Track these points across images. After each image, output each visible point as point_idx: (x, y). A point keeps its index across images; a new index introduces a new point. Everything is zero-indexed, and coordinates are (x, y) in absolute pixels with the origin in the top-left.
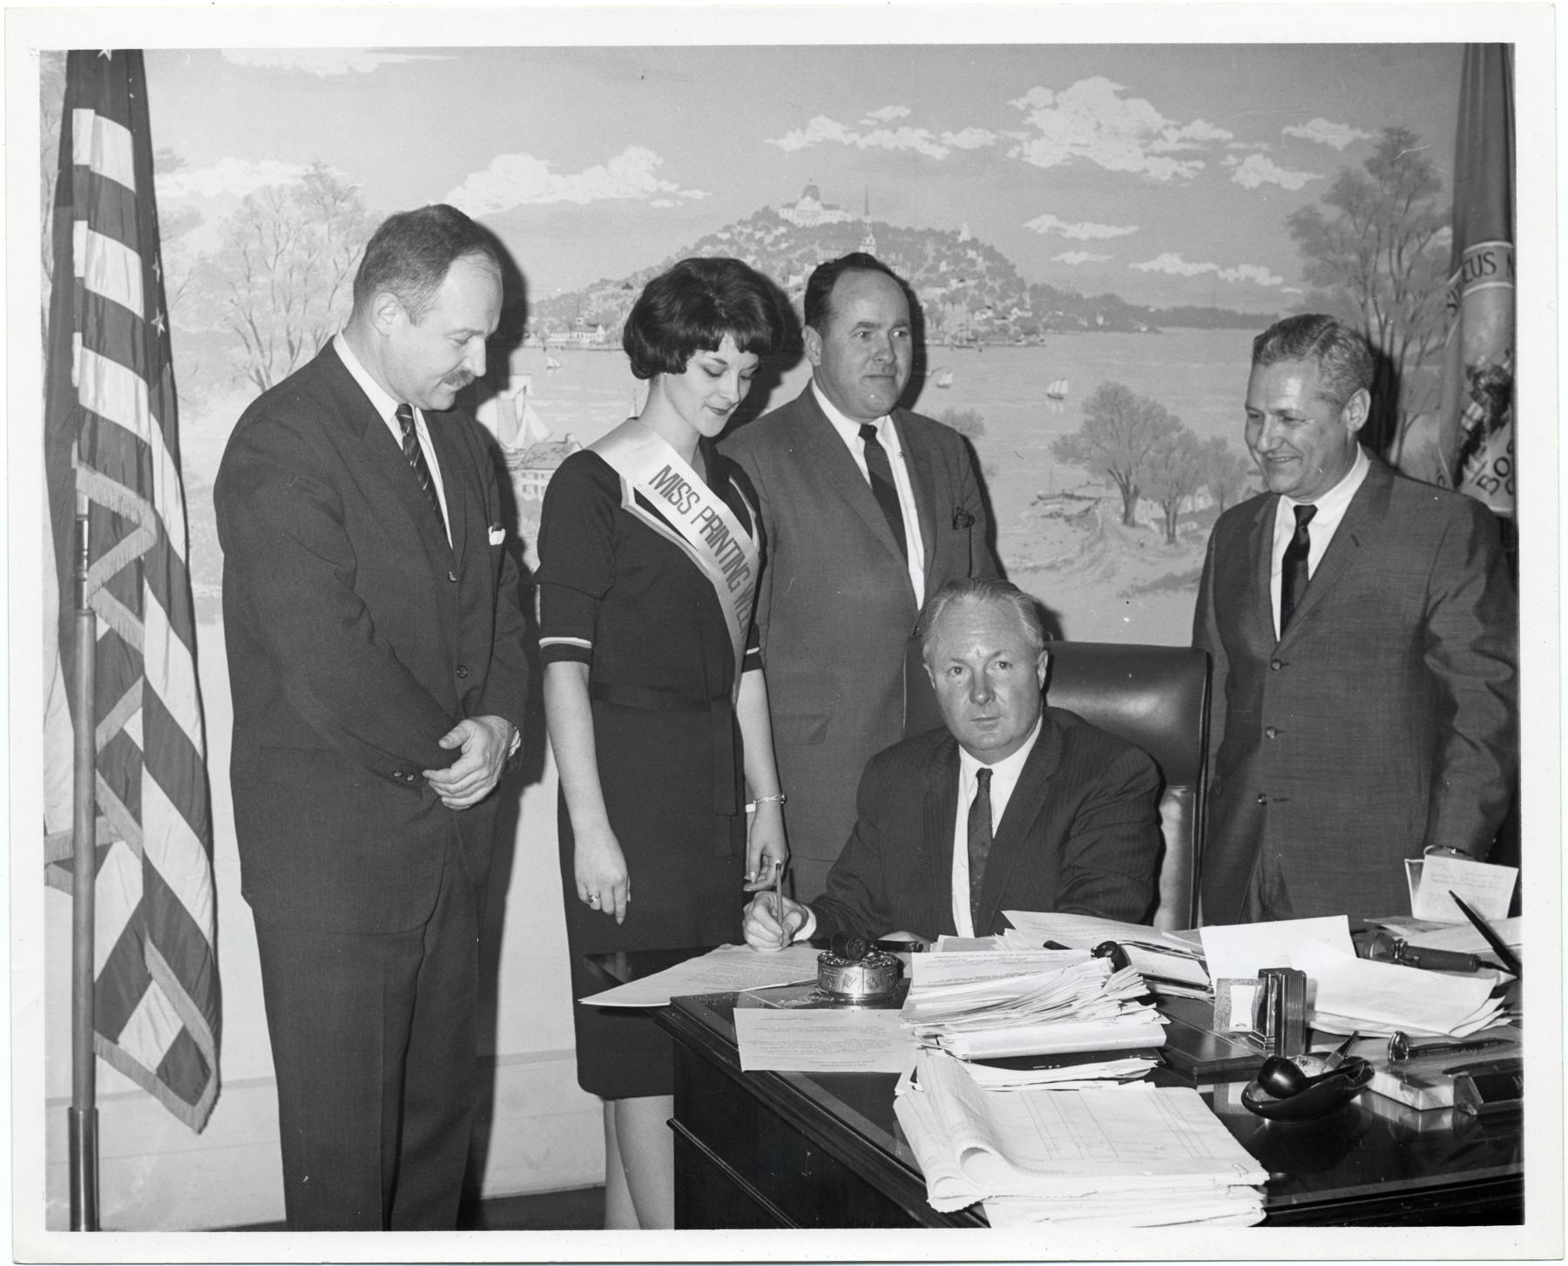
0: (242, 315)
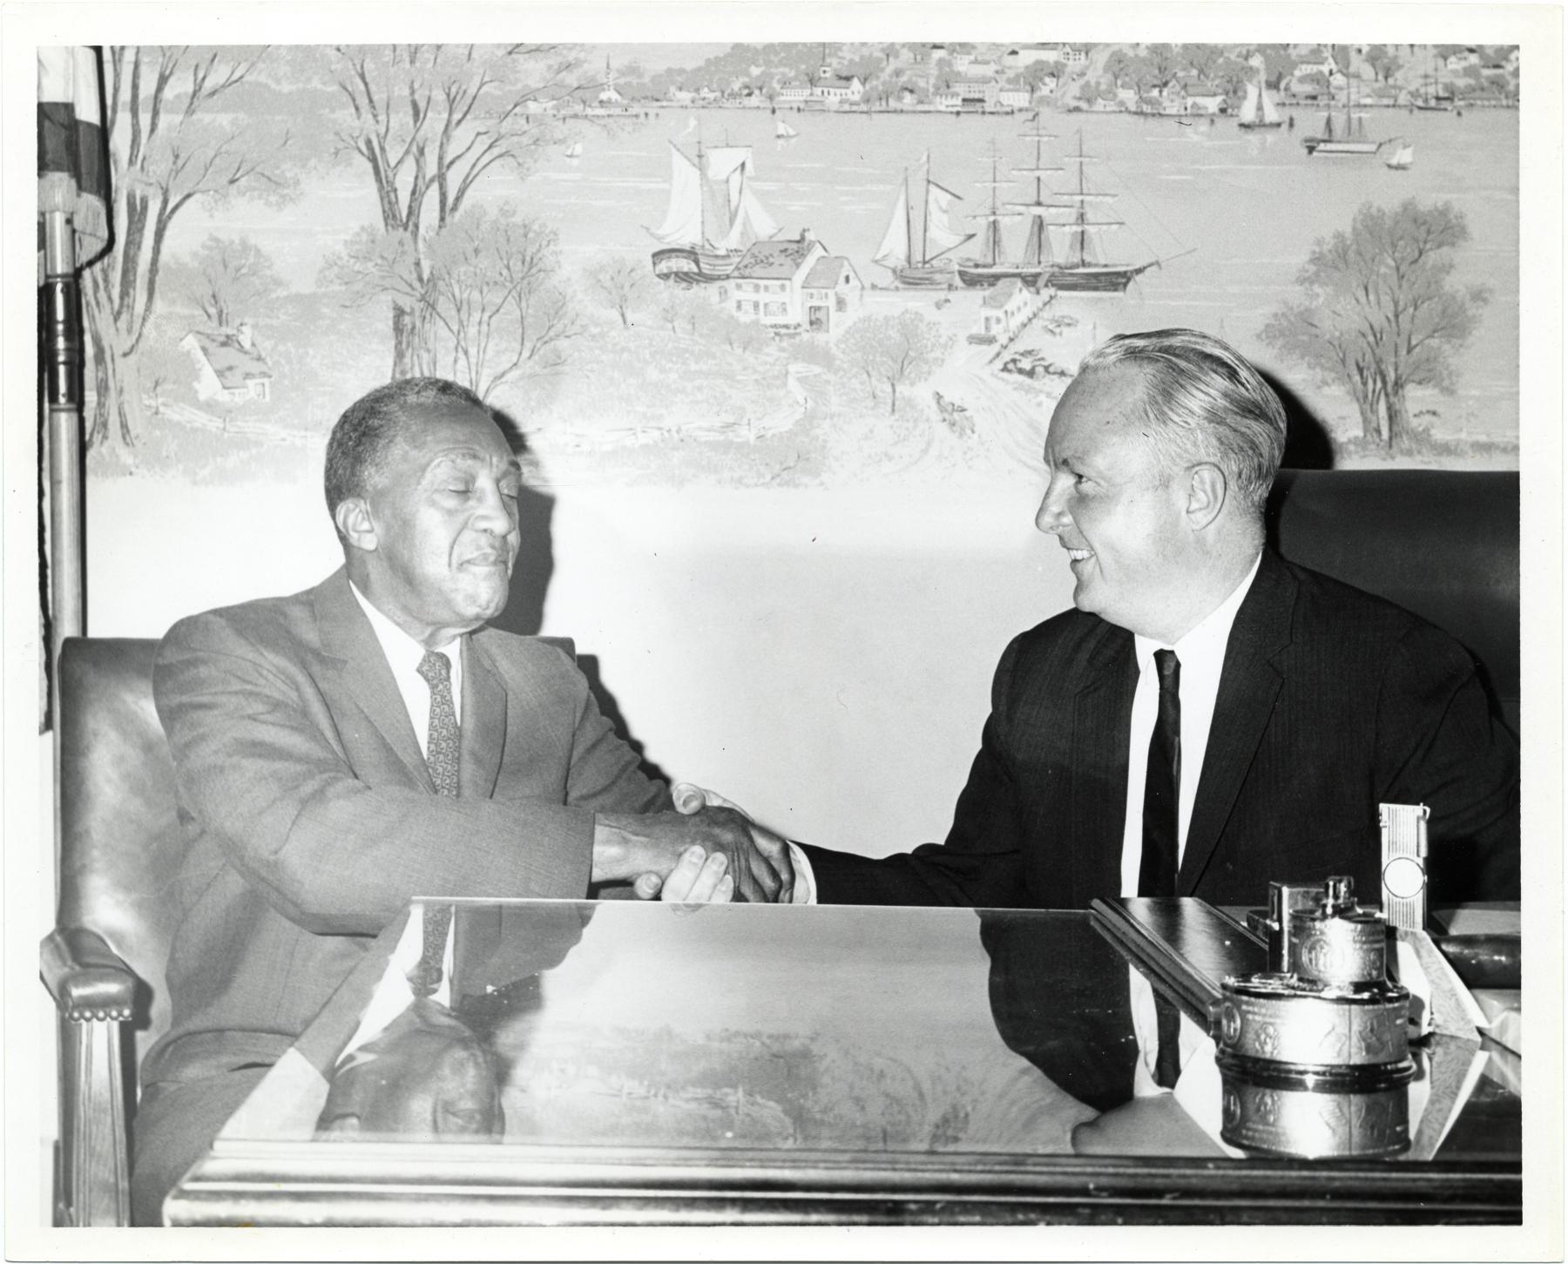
0: (351, 67)
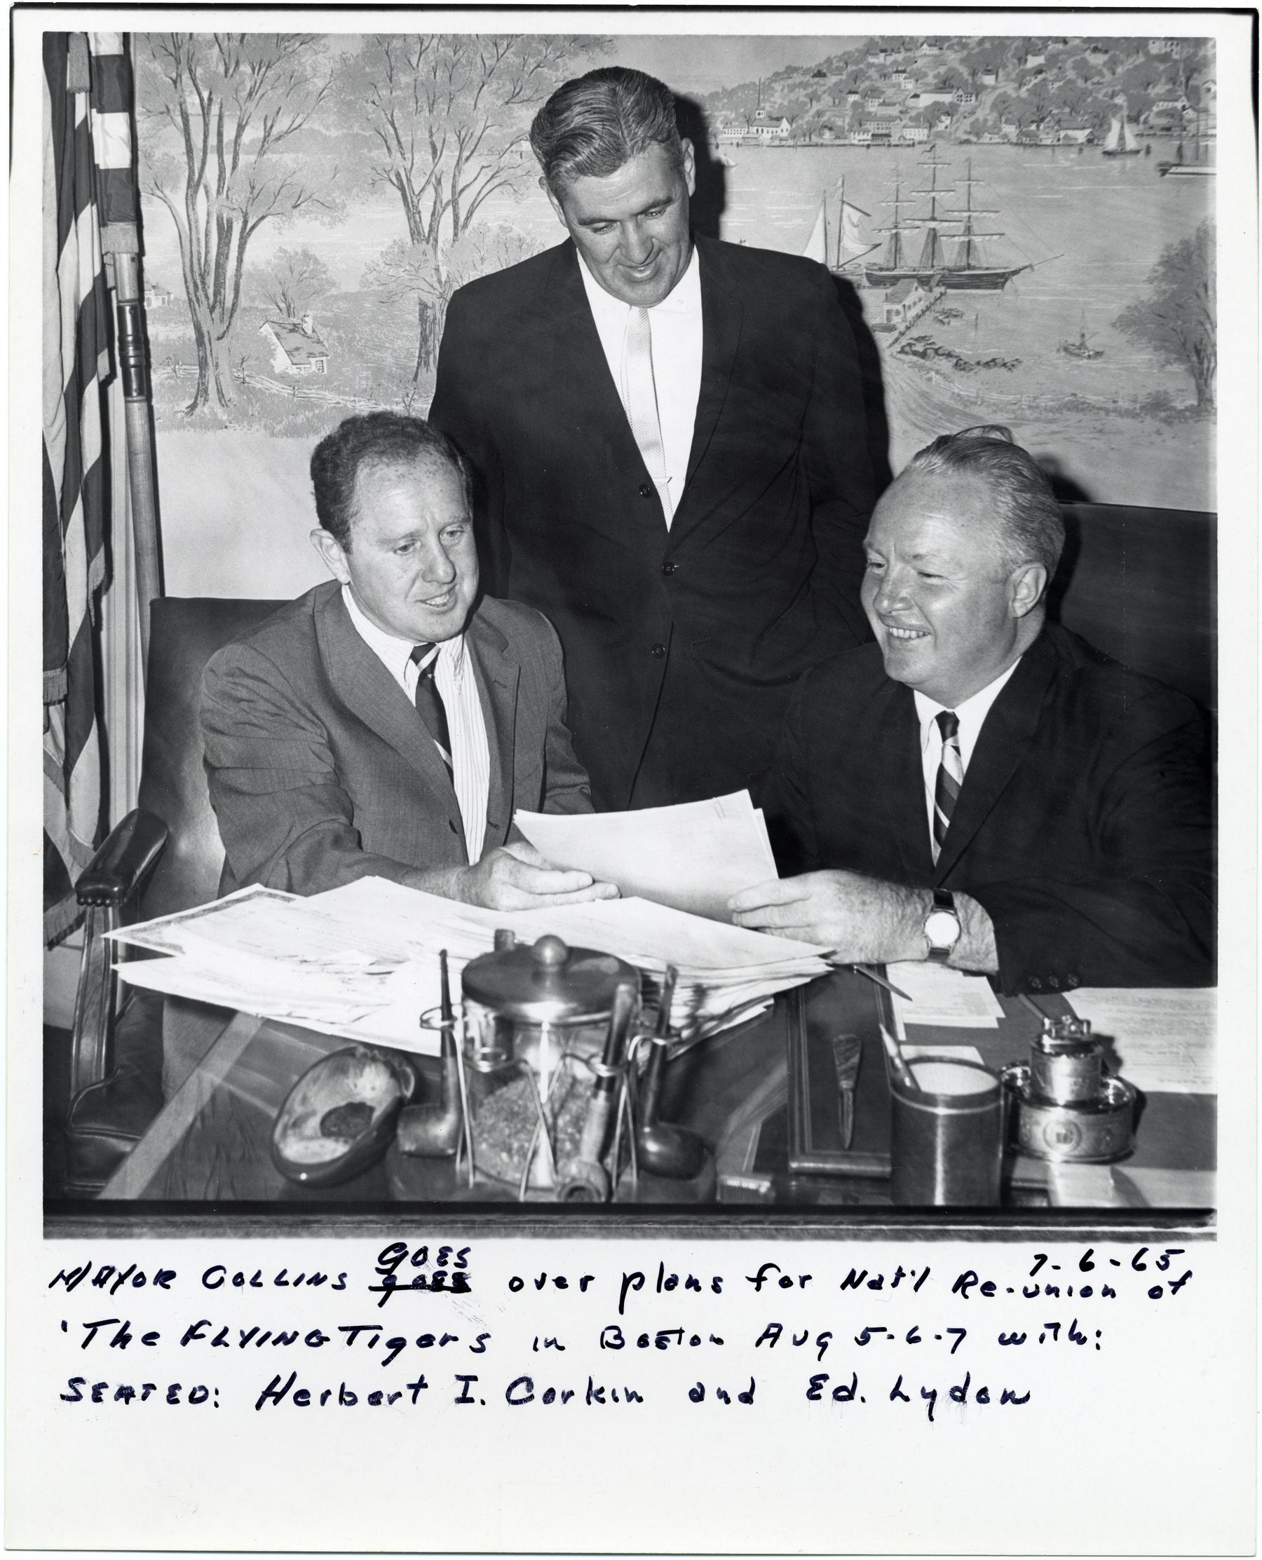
0: (383, 115)
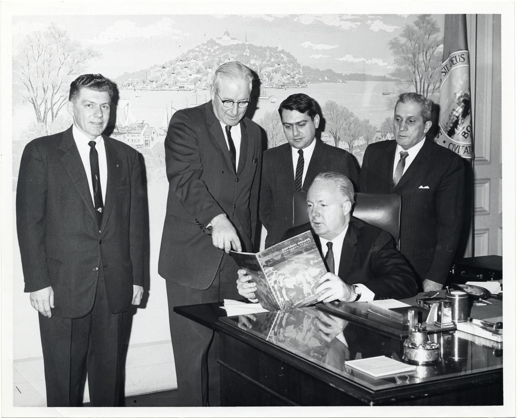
0: (26, 78)
